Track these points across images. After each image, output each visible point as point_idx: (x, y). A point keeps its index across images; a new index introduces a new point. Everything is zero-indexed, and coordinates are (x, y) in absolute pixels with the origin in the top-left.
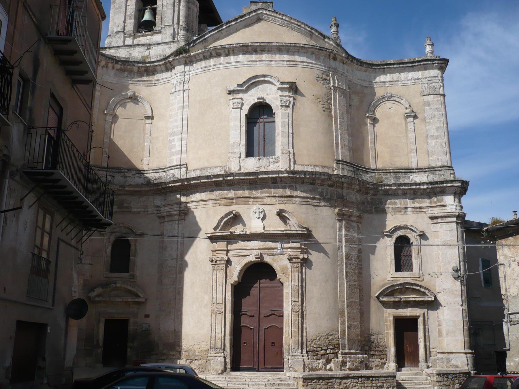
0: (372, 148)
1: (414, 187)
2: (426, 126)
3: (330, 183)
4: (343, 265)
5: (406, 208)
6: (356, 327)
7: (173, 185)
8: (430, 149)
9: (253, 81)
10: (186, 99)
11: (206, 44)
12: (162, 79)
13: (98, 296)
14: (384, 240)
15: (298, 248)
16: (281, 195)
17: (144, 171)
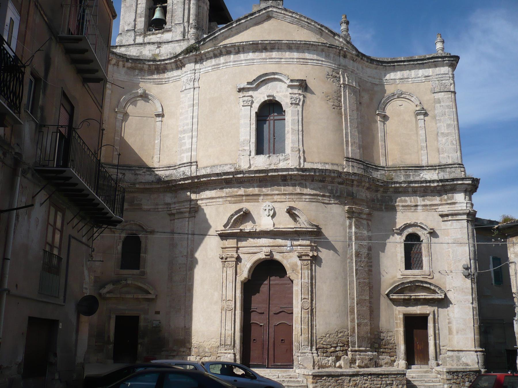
0: (382, 146)
1: (424, 185)
2: (436, 124)
3: (340, 180)
4: (353, 263)
5: (416, 206)
6: (366, 325)
7: (183, 182)
8: (441, 146)
9: (263, 79)
10: (196, 97)
11: (217, 42)
12: (172, 77)
13: (109, 292)
14: (394, 238)
15: (308, 246)
16: (291, 192)
17: (155, 168)
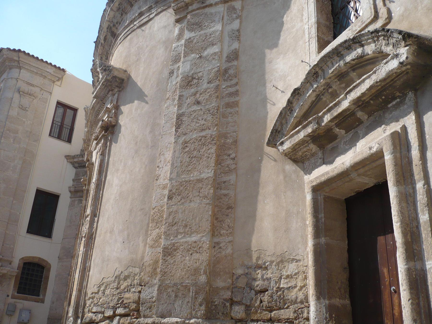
6: (194, 249)
